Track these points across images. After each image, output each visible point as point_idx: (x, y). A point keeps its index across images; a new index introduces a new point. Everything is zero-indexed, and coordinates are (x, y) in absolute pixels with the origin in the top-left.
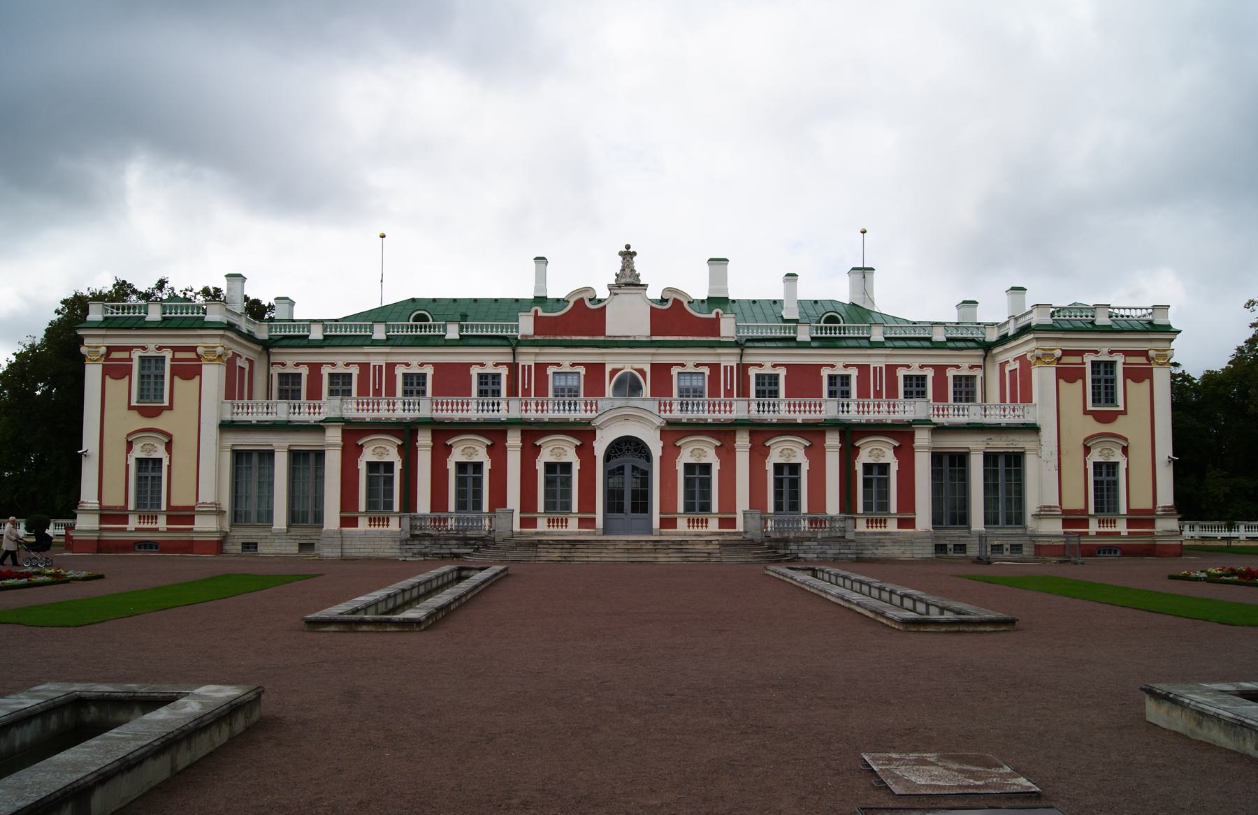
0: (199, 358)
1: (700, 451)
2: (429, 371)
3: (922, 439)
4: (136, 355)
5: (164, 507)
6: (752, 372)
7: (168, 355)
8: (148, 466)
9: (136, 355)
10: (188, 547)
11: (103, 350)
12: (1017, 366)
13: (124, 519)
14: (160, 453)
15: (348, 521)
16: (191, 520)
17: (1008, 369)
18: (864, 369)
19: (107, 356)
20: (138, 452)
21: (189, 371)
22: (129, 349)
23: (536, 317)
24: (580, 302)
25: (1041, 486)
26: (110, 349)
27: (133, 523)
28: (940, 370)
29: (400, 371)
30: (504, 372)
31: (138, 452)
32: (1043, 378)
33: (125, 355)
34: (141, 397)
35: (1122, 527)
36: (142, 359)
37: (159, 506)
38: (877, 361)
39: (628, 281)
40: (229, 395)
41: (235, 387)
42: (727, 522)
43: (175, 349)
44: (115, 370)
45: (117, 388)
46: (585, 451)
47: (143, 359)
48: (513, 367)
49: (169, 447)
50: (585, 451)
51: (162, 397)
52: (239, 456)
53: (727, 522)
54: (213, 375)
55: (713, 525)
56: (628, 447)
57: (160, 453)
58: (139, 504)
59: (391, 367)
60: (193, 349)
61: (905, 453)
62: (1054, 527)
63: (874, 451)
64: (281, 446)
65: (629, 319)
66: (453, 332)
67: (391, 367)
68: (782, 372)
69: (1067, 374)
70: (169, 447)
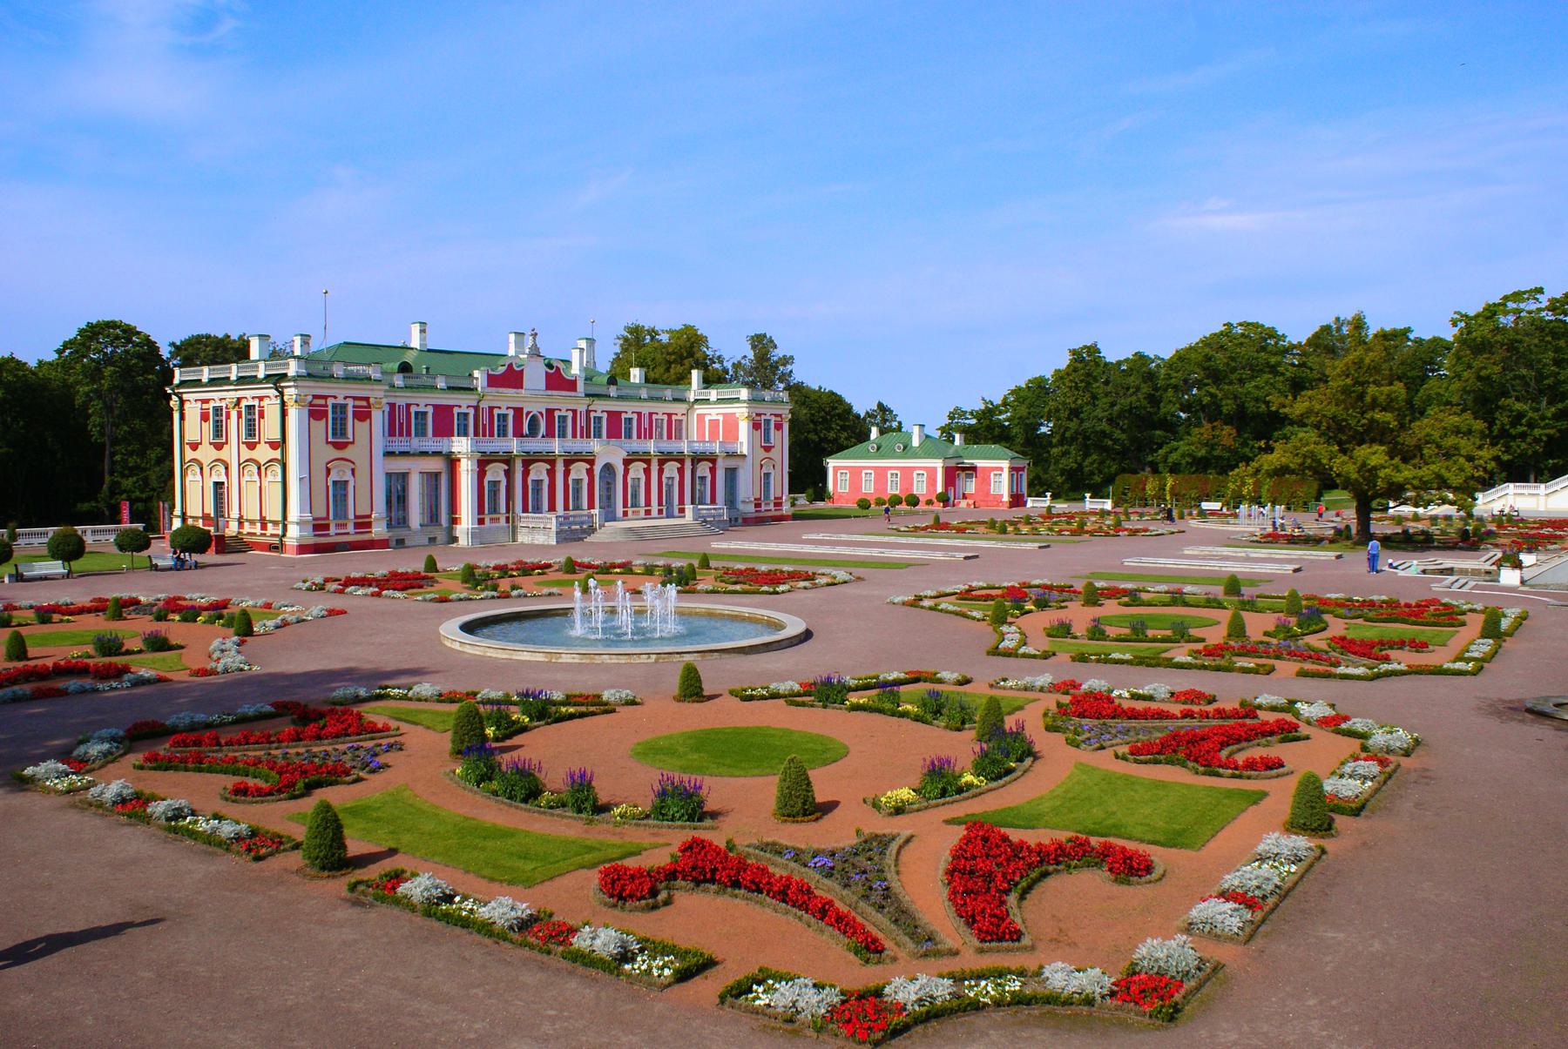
0: (369, 406)
1: (637, 470)
2: (430, 410)
3: (721, 466)
4: (330, 401)
5: (351, 516)
6: (592, 415)
7: (350, 403)
8: (341, 486)
9: (330, 401)
10: (371, 544)
11: (310, 398)
12: (721, 418)
13: (327, 527)
14: (348, 476)
15: (481, 521)
16: (369, 525)
17: (707, 418)
18: (639, 414)
19: (311, 404)
20: (334, 477)
21: (363, 415)
22: (325, 397)
23: (489, 376)
24: (510, 366)
25: (747, 489)
26: (315, 397)
27: (333, 530)
28: (670, 415)
29: (413, 409)
30: (472, 411)
31: (334, 477)
32: (744, 428)
33: (322, 402)
34: (334, 434)
35: (772, 507)
36: (335, 406)
37: (346, 517)
38: (645, 408)
39: (535, 353)
40: (392, 433)
41: (392, 430)
42: (648, 512)
43: (355, 398)
44: (316, 413)
45: (319, 426)
46: (590, 472)
47: (335, 406)
48: (476, 408)
49: (353, 471)
50: (590, 472)
51: (344, 434)
52: (389, 475)
53: (648, 512)
54: (378, 418)
55: (642, 514)
56: (608, 468)
57: (348, 476)
58: (335, 515)
59: (408, 406)
60: (367, 399)
61: (713, 471)
62: (751, 508)
63: (704, 469)
64: (416, 470)
65: (535, 377)
66: (441, 384)
67: (408, 406)
68: (605, 416)
69: (756, 426)
70: (353, 471)
